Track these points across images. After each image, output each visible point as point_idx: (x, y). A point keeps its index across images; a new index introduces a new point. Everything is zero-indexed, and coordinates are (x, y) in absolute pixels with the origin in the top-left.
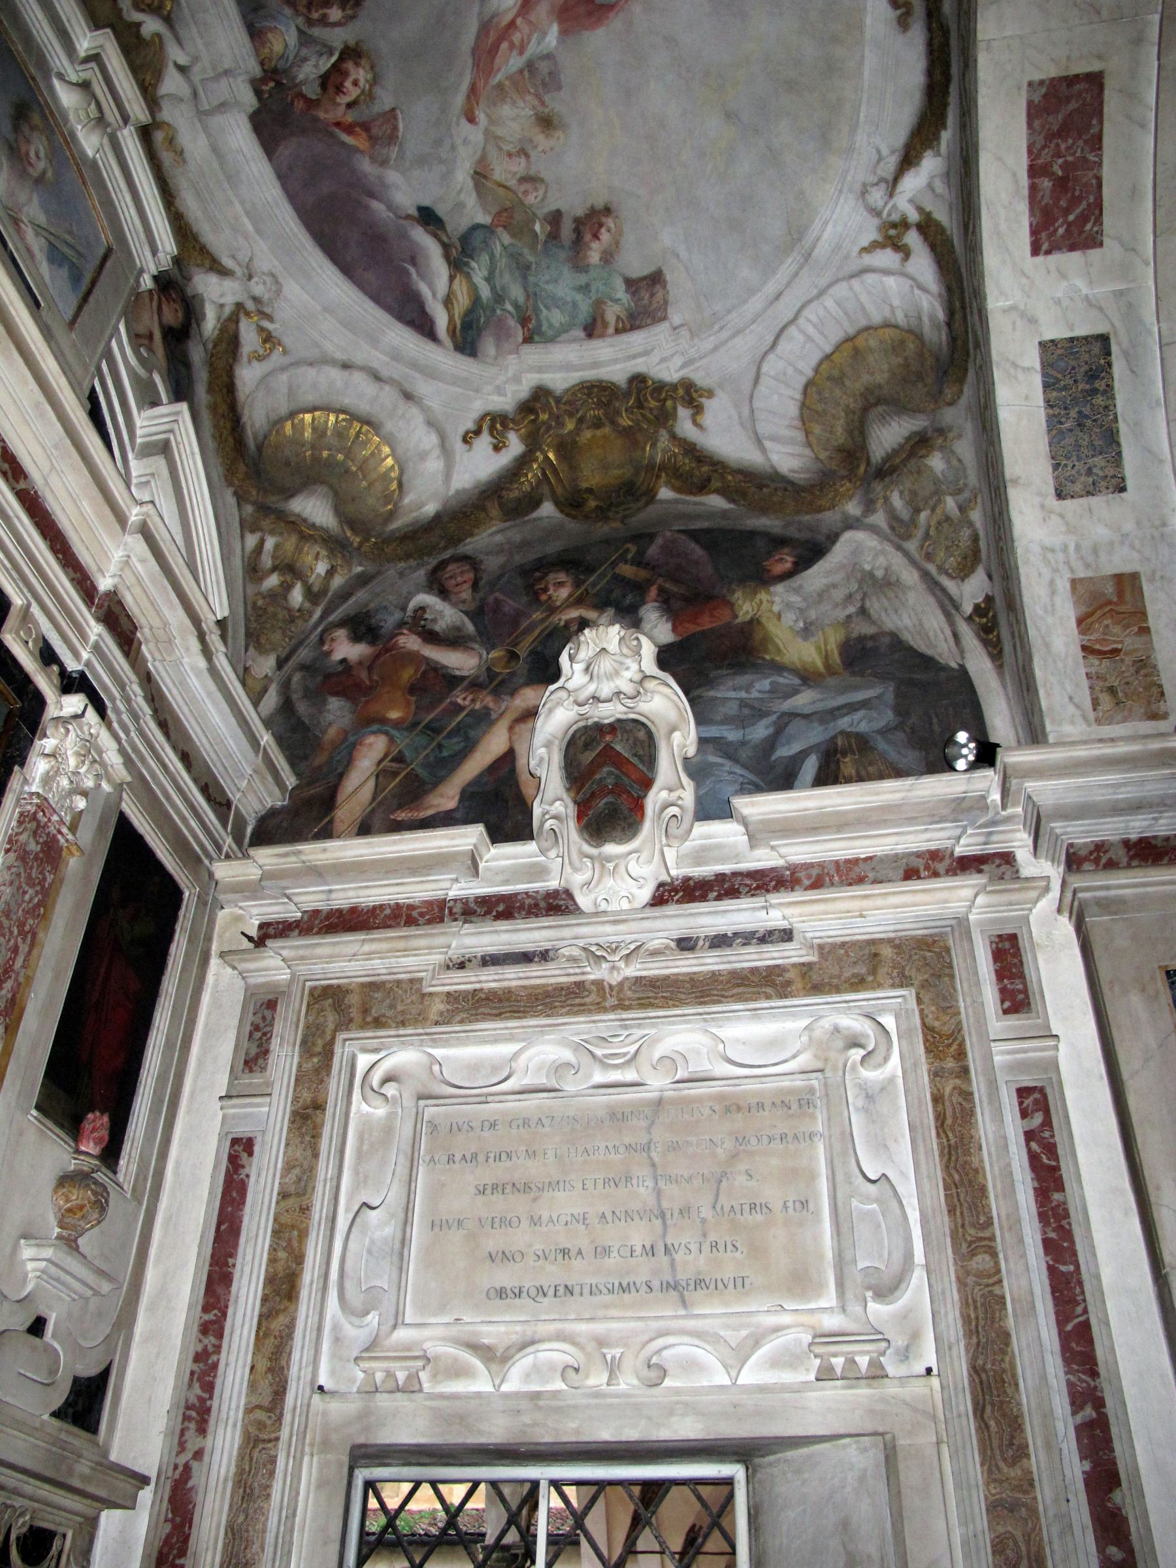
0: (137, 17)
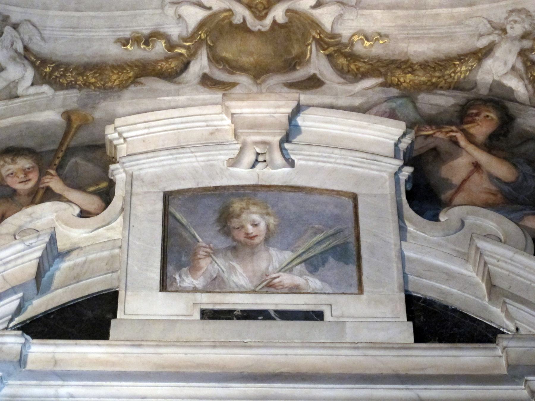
0: (268, 21)
